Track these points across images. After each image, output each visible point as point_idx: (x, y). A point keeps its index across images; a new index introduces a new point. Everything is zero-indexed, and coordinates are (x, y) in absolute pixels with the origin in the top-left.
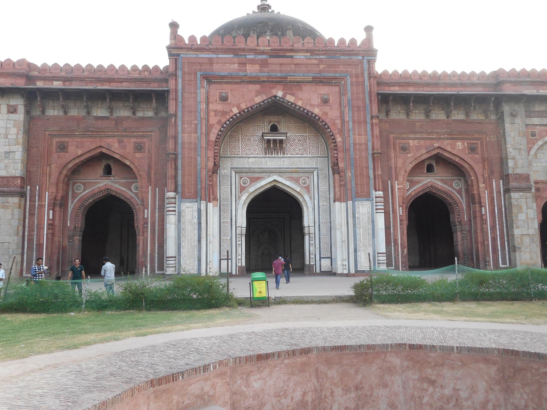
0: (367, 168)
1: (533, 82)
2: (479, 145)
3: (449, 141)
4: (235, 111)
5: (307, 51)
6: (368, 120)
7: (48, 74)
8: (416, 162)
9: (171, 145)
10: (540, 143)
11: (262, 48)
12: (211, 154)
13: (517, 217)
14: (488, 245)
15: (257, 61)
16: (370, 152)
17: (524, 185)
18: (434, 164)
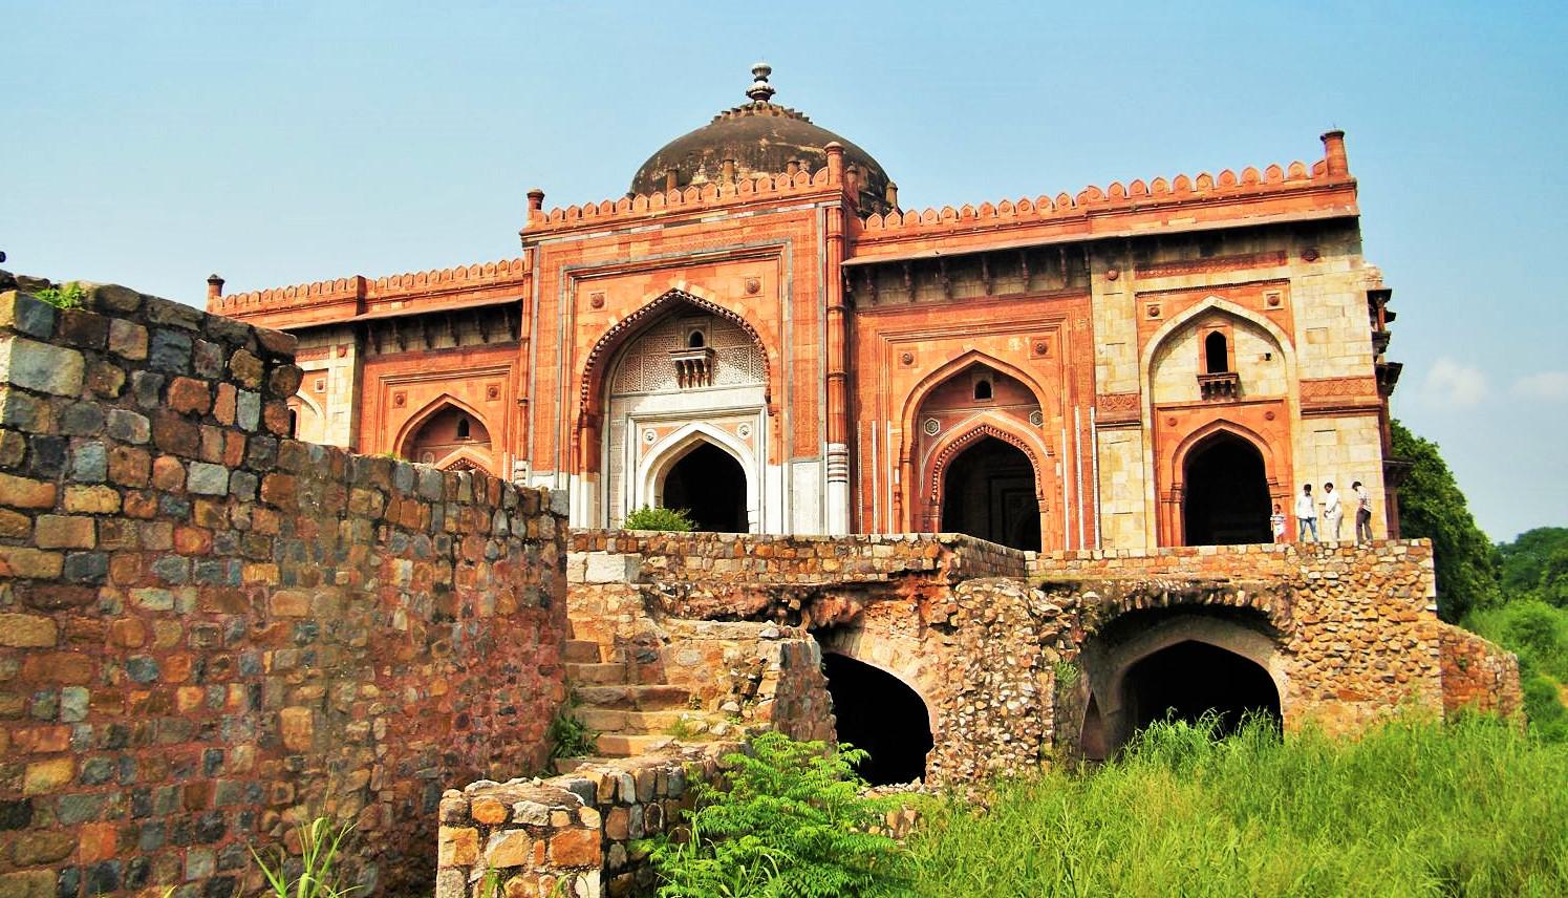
0: (815, 402)
1: (1152, 205)
2: (1055, 342)
3: (994, 337)
4: (614, 322)
5: (723, 207)
6: (821, 317)
7: (386, 294)
8: (932, 383)
9: (522, 388)
10: (1168, 328)
11: (653, 214)
12: (577, 396)
13: (1109, 479)
14: (1063, 536)
15: (645, 235)
16: (822, 374)
17: (1123, 415)
18: (991, 381)
